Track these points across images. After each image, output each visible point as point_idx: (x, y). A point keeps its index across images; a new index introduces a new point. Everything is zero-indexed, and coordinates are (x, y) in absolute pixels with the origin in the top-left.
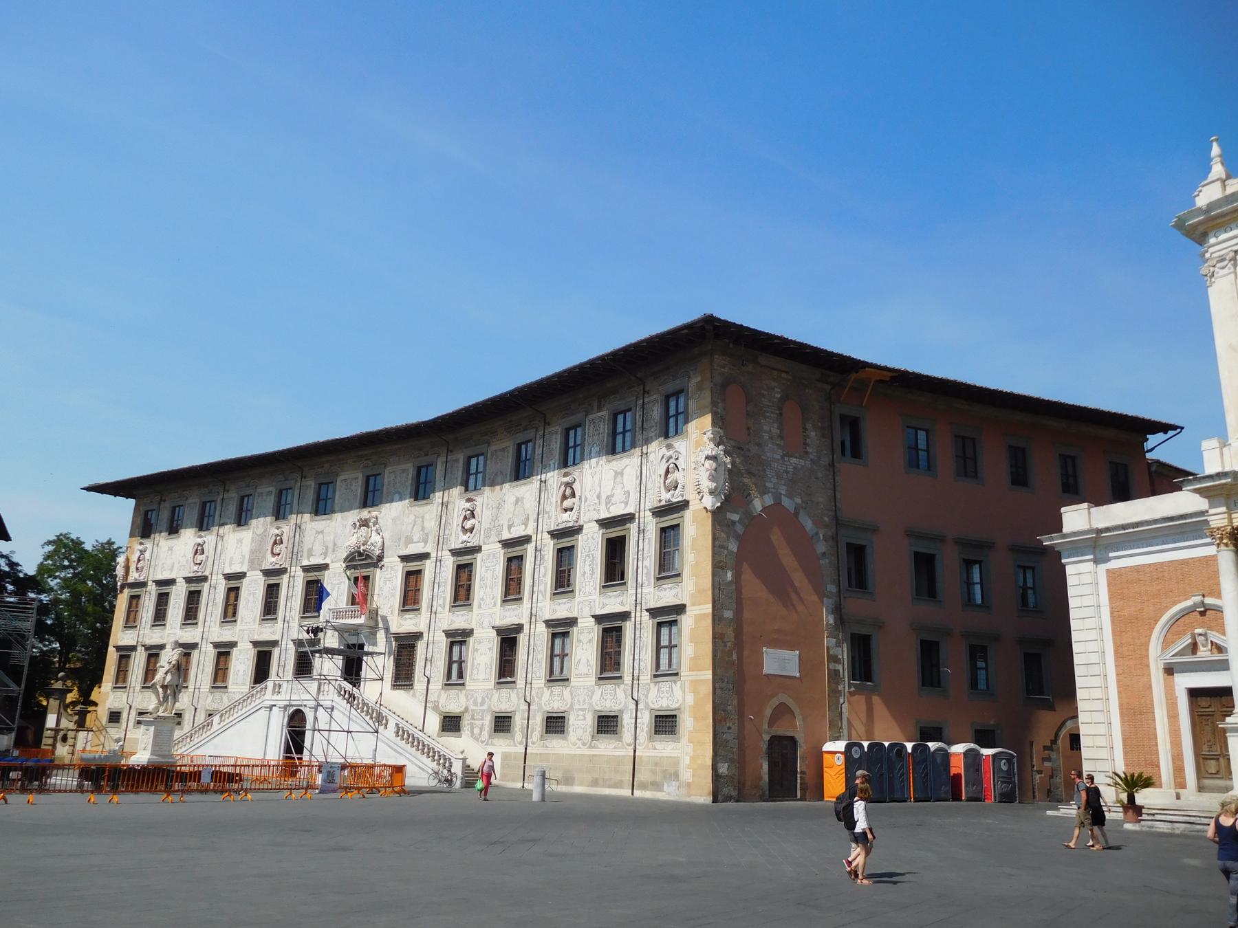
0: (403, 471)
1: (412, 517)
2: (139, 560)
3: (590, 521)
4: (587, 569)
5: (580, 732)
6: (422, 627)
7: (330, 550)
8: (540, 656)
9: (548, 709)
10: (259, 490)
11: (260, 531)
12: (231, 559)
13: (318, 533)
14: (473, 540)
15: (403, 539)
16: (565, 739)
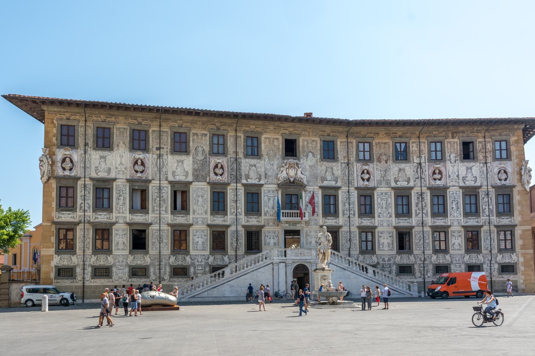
0: (313, 141)
1: (324, 167)
3: (453, 186)
4: (454, 206)
7: (263, 177)
11: (200, 157)
12: (174, 173)
13: (250, 165)
14: (371, 184)
15: (319, 178)
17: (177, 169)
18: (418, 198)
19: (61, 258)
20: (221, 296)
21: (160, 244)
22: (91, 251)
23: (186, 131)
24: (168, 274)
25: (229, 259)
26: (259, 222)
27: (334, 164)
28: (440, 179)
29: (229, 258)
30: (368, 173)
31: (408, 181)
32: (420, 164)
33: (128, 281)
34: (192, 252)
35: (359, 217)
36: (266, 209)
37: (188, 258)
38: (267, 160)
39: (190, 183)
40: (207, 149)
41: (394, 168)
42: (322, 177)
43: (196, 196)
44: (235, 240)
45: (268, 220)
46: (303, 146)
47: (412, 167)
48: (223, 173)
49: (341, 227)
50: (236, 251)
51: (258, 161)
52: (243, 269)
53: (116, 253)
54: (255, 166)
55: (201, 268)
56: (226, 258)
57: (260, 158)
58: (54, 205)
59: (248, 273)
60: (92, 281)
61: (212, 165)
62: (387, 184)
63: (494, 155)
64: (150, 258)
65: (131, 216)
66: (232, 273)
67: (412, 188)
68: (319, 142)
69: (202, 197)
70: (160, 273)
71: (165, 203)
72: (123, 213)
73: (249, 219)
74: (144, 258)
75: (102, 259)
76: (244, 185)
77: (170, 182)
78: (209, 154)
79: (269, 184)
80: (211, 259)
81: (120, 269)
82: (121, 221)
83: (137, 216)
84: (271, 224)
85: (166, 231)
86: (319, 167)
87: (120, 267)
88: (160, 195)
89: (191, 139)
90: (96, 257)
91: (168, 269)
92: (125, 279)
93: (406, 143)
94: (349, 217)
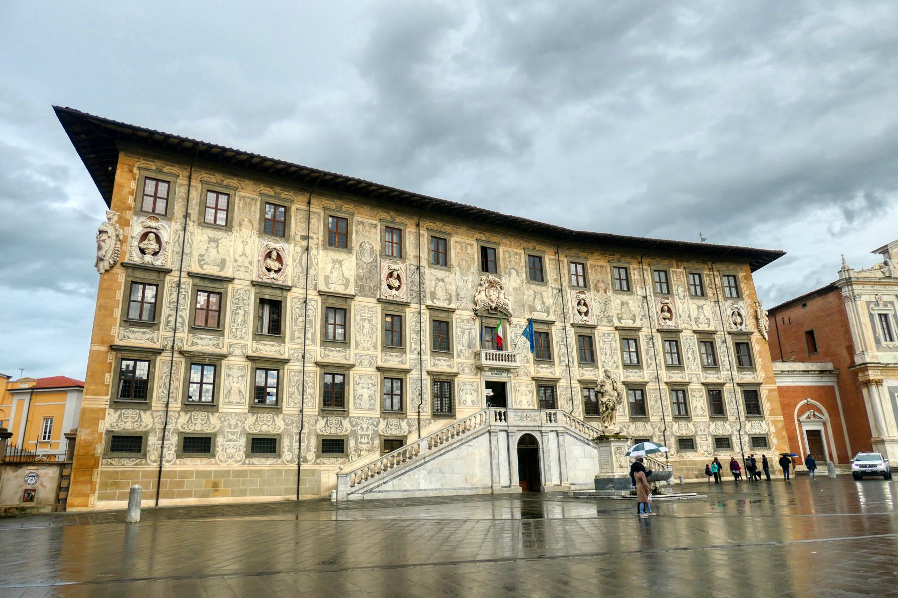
0: (516, 254)
1: (531, 292)
2: (145, 236)
4: (690, 356)
5: (705, 448)
6: (557, 375)
7: (454, 298)
8: (664, 403)
9: (678, 434)
10: (358, 218)
11: (367, 259)
12: (327, 278)
13: (437, 279)
15: (526, 307)
16: (696, 451)
17: (332, 273)
18: (648, 343)
19: (120, 416)
20: (414, 488)
21: (301, 395)
22: (179, 405)
23: (346, 216)
24: (313, 450)
25: (409, 425)
26: (450, 366)
27: (543, 288)
28: (670, 319)
29: (408, 423)
30: (585, 304)
31: (634, 319)
32: (646, 297)
33: (244, 463)
34: (353, 413)
35: (579, 367)
36: (460, 347)
37: (346, 423)
38: (458, 273)
39: (352, 297)
40: (377, 247)
41: (616, 300)
42: (530, 306)
43: (361, 319)
44: (419, 394)
45: (462, 364)
46: (504, 259)
47: (636, 301)
48: (399, 286)
49: (557, 380)
50: (419, 412)
51: (447, 273)
52: (447, 440)
53: (224, 410)
54: (443, 280)
55: (366, 441)
56: (404, 424)
57: (449, 271)
58: (118, 313)
59: (455, 448)
60: (178, 461)
61: (385, 272)
62: (609, 322)
63: (724, 293)
64: (284, 421)
65: (255, 345)
66: (430, 448)
67: (638, 329)
68: (523, 256)
69: (370, 321)
70: (299, 448)
71: (311, 327)
72: (242, 338)
73: (436, 362)
74: (274, 420)
75: (199, 421)
76: (428, 307)
77: (321, 293)
78: (380, 255)
79: (462, 309)
80: (383, 424)
81: (230, 440)
82: (238, 352)
83: (265, 345)
84: (467, 370)
85: (311, 375)
86: (525, 291)
87: (230, 437)
88: (302, 315)
89: (354, 229)
90: (189, 415)
91: (314, 442)
92: (238, 459)
93: (626, 269)
94: (568, 366)
